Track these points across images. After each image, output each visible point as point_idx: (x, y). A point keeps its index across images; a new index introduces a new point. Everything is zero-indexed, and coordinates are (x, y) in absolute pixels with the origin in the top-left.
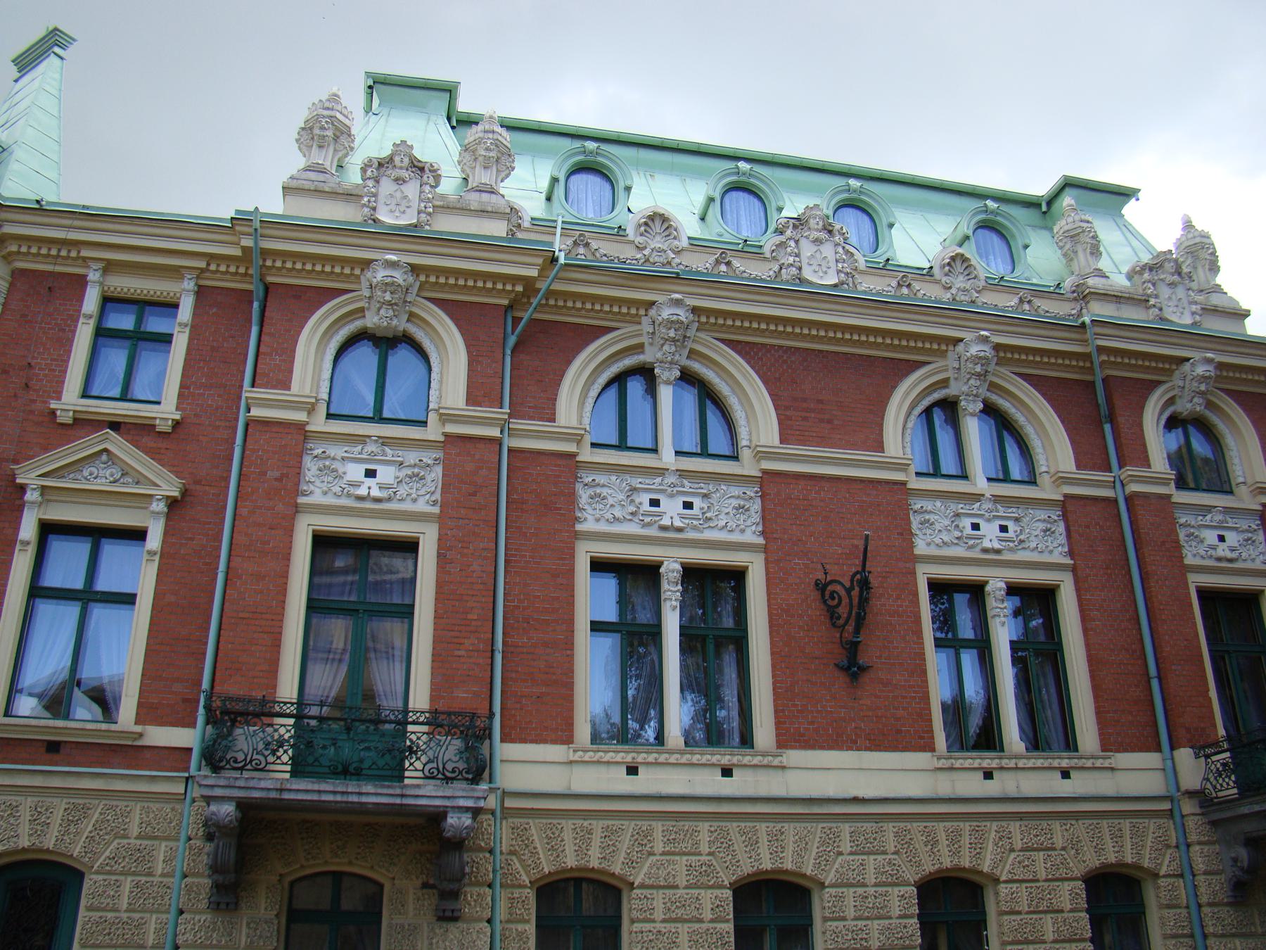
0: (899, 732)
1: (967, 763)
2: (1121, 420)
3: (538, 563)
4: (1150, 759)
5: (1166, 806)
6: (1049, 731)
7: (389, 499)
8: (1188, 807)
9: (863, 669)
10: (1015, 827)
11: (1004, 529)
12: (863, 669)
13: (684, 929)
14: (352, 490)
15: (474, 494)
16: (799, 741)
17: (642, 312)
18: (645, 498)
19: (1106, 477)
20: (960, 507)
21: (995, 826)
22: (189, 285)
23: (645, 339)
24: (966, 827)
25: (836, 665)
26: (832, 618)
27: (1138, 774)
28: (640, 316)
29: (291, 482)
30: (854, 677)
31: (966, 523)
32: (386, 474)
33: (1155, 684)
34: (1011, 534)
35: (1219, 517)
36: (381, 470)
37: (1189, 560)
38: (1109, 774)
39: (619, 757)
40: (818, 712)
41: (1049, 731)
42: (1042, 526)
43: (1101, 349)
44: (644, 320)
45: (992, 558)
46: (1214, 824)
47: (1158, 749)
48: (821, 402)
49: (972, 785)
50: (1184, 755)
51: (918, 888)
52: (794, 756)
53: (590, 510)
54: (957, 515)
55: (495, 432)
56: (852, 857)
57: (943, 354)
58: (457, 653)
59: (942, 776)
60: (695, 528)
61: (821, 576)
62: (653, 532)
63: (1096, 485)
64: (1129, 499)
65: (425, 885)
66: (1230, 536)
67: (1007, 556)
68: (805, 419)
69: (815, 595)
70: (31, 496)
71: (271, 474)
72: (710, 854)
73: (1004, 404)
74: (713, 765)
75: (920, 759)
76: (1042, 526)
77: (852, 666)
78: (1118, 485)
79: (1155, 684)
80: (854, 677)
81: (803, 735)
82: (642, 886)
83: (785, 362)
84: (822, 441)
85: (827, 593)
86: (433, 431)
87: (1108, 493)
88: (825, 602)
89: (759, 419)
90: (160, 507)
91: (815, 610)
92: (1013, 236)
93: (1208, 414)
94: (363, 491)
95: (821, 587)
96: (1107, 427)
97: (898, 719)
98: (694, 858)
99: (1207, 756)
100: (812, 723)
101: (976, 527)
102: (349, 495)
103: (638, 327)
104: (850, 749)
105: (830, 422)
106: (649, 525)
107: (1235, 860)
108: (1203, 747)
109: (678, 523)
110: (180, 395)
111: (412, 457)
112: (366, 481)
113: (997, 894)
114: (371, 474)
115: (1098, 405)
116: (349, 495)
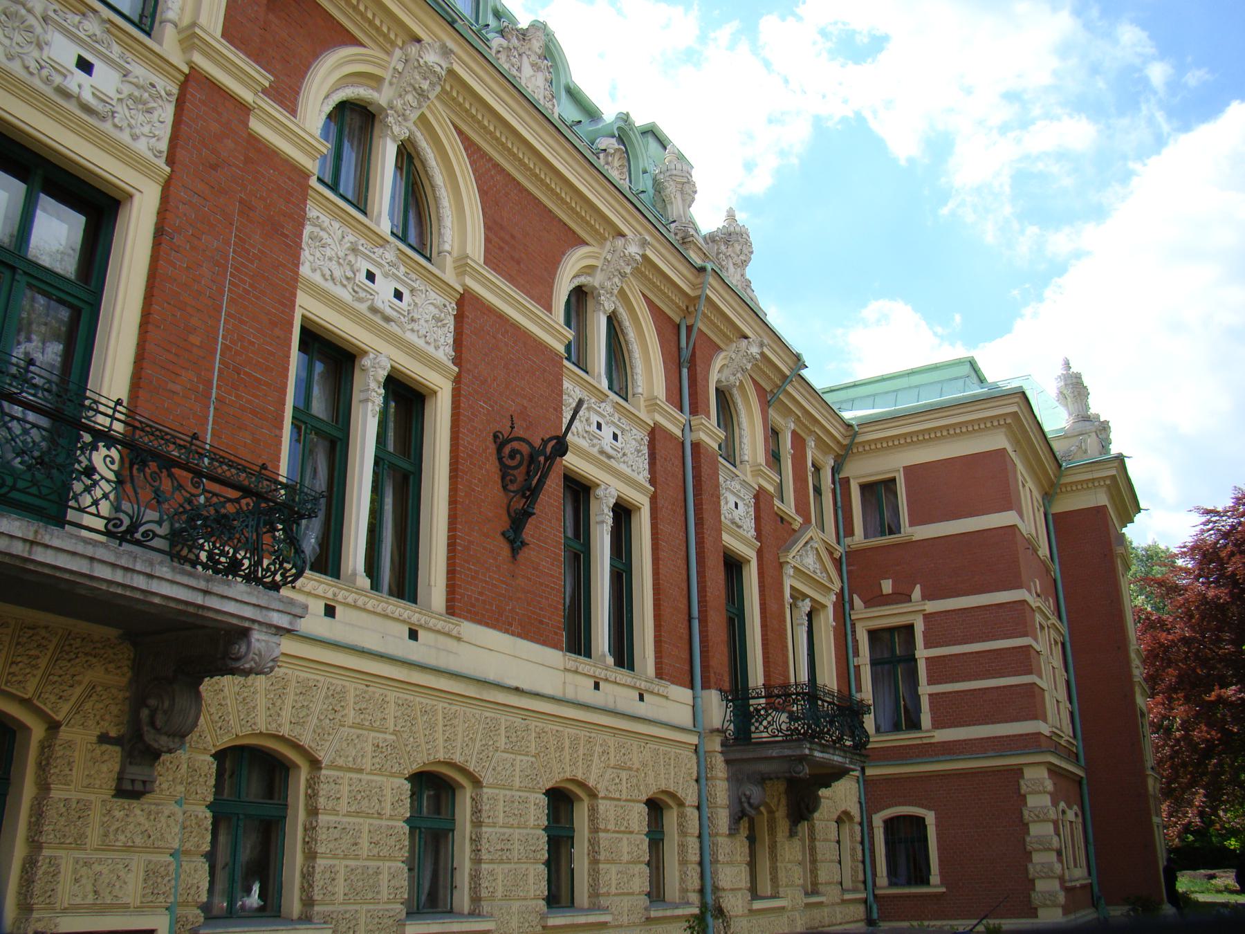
0: (541, 622)
3: (258, 298)
7: (103, 119)
8: (716, 744)
9: (523, 544)
12: (523, 544)
13: (365, 824)
15: (214, 167)
16: (470, 612)
17: (400, 43)
18: (364, 266)
19: (683, 418)
23: (387, 76)
25: (503, 534)
26: (503, 478)
27: (675, 704)
28: (393, 44)
32: (105, 79)
33: (696, 623)
35: (738, 487)
36: (99, 66)
38: (663, 700)
39: (320, 591)
40: (486, 582)
43: (708, 297)
44: (398, 53)
46: (727, 762)
47: (692, 688)
48: (513, 237)
49: (582, 689)
50: (714, 697)
52: (469, 629)
53: (307, 253)
55: (247, 96)
56: (505, 755)
57: (602, 239)
58: (171, 386)
60: (400, 325)
61: (506, 430)
62: (363, 307)
65: (103, 739)
66: (740, 505)
67: (613, 463)
68: (501, 249)
69: (492, 448)
72: (395, 733)
73: (623, 314)
74: (404, 621)
78: (687, 427)
79: (696, 623)
81: (473, 606)
82: (333, 767)
83: (492, 177)
84: (511, 280)
85: (507, 450)
88: (500, 459)
89: (462, 225)
91: (492, 466)
93: (735, 391)
95: (500, 442)
96: (685, 371)
97: (541, 609)
98: (381, 736)
100: (481, 594)
102: (47, 81)
103: (385, 57)
104: (506, 632)
105: (518, 263)
106: (360, 300)
109: (389, 311)
111: (140, 72)
114: (85, 66)
115: (679, 349)
116: (47, 81)
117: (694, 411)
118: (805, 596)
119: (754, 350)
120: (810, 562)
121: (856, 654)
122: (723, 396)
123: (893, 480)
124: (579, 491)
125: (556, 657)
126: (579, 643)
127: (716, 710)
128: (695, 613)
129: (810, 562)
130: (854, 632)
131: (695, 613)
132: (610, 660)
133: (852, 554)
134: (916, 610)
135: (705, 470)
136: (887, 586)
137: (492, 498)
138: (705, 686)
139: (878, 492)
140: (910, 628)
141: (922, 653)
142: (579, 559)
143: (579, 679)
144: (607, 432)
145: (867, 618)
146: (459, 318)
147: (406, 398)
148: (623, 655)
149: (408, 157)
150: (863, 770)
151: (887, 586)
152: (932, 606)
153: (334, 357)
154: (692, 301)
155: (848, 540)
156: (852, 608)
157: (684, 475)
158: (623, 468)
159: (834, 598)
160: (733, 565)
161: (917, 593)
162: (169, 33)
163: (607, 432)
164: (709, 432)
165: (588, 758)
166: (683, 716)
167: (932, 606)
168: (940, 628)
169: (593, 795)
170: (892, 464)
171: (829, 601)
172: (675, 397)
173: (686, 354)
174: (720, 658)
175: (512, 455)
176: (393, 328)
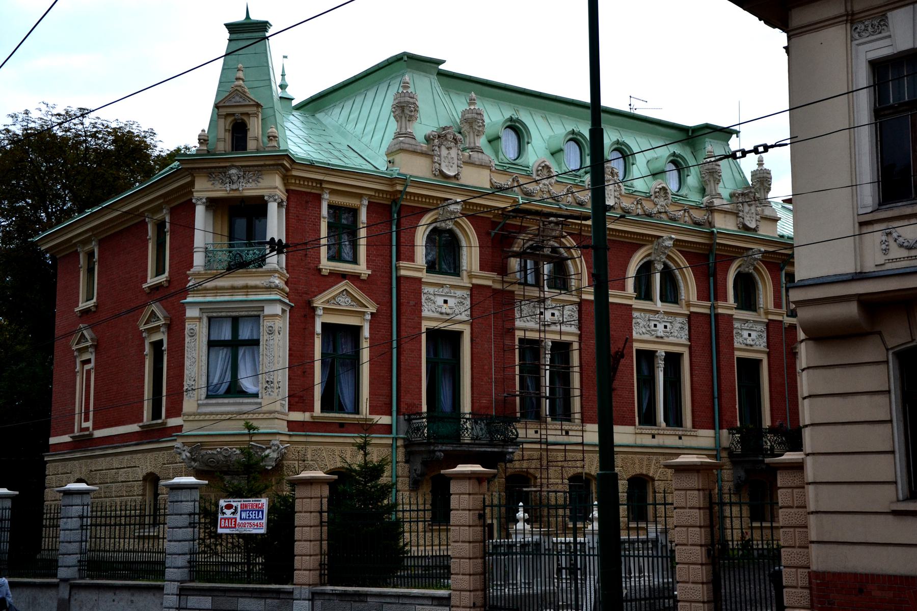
1: (647, 432)
2: (718, 277)
4: (711, 433)
5: (715, 453)
6: (674, 418)
10: (661, 458)
11: (666, 327)
14: (439, 309)
19: (708, 304)
20: (651, 316)
21: (655, 457)
22: (366, 202)
24: (646, 457)
27: (705, 437)
29: (419, 305)
31: (652, 324)
32: (452, 302)
33: (716, 400)
34: (668, 329)
36: (449, 300)
37: (736, 345)
38: (695, 438)
41: (674, 418)
42: (679, 325)
45: (659, 340)
47: (714, 428)
49: (647, 440)
50: (725, 432)
51: (628, 480)
54: (649, 320)
57: (652, 242)
59: (638, 436)
63: (702, 308)
67: (666, 340)
70: (319, 312)
71: (412, 303)
75: (630, 429)
76: (679, 325)
79: (716, 400)
86: (466, 282)
90: (368, 317)
94: (444, 311)
99: (733, 434)
101: (655, 326)
107: (740, 477)
108: (732, 429)
110: (368, 261)
111: (459, 293)
112: (445, 304)
113: (653, 485)
117: (716, 299)
126: (648, 418)
128: (716, 394)
131: (716, 394)
132: (663, 424)
135: (722, 326)
138: (721, 428)
143: (642, 436)
144: (660, 327)
146: (580, 312)
147: (561, 349)
154: (710, 246)
157: (709, 332)
158: (672, 339)
162: (465, 274)
163: (660, 327)
164: (728, 306)
165: (648, 465)
169: (653, 479)
172: (703, 295)
173: (712, 270)
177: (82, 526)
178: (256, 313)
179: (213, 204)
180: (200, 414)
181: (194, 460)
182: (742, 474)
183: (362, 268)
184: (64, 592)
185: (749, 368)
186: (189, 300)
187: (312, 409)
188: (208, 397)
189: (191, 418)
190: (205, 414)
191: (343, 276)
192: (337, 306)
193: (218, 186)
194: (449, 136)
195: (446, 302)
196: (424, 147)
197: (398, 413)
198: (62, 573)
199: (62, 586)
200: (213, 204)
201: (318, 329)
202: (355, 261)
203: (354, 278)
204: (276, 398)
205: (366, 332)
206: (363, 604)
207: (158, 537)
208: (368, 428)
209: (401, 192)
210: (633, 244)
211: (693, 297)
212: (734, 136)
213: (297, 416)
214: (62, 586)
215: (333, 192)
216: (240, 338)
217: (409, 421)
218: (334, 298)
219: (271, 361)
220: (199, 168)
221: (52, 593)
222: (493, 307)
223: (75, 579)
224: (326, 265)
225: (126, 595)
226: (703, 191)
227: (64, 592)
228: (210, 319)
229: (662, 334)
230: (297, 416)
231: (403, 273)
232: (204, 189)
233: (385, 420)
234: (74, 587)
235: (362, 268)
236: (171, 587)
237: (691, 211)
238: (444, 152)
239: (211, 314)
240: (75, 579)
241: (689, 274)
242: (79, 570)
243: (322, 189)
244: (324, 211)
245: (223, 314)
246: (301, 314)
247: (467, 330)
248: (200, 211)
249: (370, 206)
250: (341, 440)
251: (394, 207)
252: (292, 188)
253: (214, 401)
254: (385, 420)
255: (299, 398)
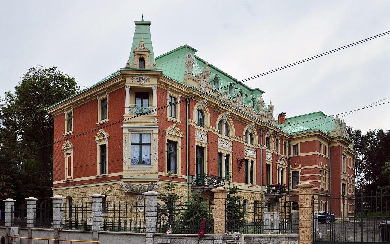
5: (261, 193)
18: (223, 143)
19: (260, 145)
27: (259, 188)
30: (239, 172)
43: (265, 127)
47: (261, 185)
49: (247, 188)
57: (249, 123)
64: (263, 149)
70: (167, 135)
77: (239, 172)
80: (239, 172)
87: (260, 148)
90: (181, 139)
91: (237, 163)
92: (255, 101)
117: (263, 144)
118: (281, 167)
119: (273, 131)
120: (282, 162)
121: (290, 176)
122: (268, 139)
123: (298, 145)
124: (247, 161)
125: (244, 184)
126: (246, 182)
127: (264, 188)
129: (282, 162)
130: (290, 172)
133: (291, 158)
134: (300, 168)
136: (296, 164)
137: (236, 167)
139: (296, 147)
140: (298, 171)
141: (300, 176)
142: (246, 170)
143: (246, 187)
145: (292, 169)
148: (252, 182)
149: (226, 125)
150: (290, 195)
151: (296, 164)
152: (303, 168)
153: (221, 154)
155: (290, 156)
156: (290, 168)
157: (260, 154)
159: (286, 167)
160: (268, 166)
161: (300, 166)
164: (265, 147)
166: (260, 190)
167: (303, 168)
168: (303, 172)
170: (298, 142)
171: (285, 167)
174: (265, 181)
175: (239, 160)
176: (226, 149)
177: (61, 211)
178: (149, 133)
179: (132, 89)
180: (129, 171)
181: (128, 188)
182: (269, 200)
183: (178, 120)
184: (95, 235)
185: (268, 166)
186: (124, 126)
187: (164, 171)
188: (131, 164)
189: (126, 172)
190: (131, 171)
191: (174, 123)
192: (174, 133)
193: (135, 82)
194: (203, 76)
195: (201, 136)
196: (195, 79)
197: (189, 174)
198: (94, 228)
199: (94, 233)
200: (132, 89)
201: (167, 142)
202: (175, 117)
203: (177, 123)
204: (155, 166)
205: (179, 145)
206: (251, 241)
207: (107, 217)
208: (180, 179)
209: (191, 93)
210: (247, 122)
211: (257, 143)
212: (263, 94)
213: (161, 174)
214: (94, 233)
215: (171, 90)
216: (142, 142)
217: (192, 177)
218: (171, 130)
219: (152, 153)
220: (128, 74)
221: (90, 235)
222: (213, 140)
223: (99, 231)
224: (169, 118)
225: (126, 238)
226: (258, 109)
227: (95, 235)
228: (131, 134)
229: (250, 154)
230: (161, 174)
231: (191, 124)
232: (130, 83)
233: (184, 177)
234: (99, 233)
235: (178, 120)
236: (149, 235)
237: (258, 115)
238: (202, 82)
239: (132, 132)
240: (99, 231)
241: (257, 135)
242: (61, 226)
243: (168, 88)
244: (168, 97)
245: (137, 132)
246: (162, 134)
247: (206, 146)
248: (128, 92)
249: (181, 97)
250: (181, 184)
251: (189, 99)
252: (160, 86)
253: (134, 166)
254: (184, 177)
255: (161, 168)
